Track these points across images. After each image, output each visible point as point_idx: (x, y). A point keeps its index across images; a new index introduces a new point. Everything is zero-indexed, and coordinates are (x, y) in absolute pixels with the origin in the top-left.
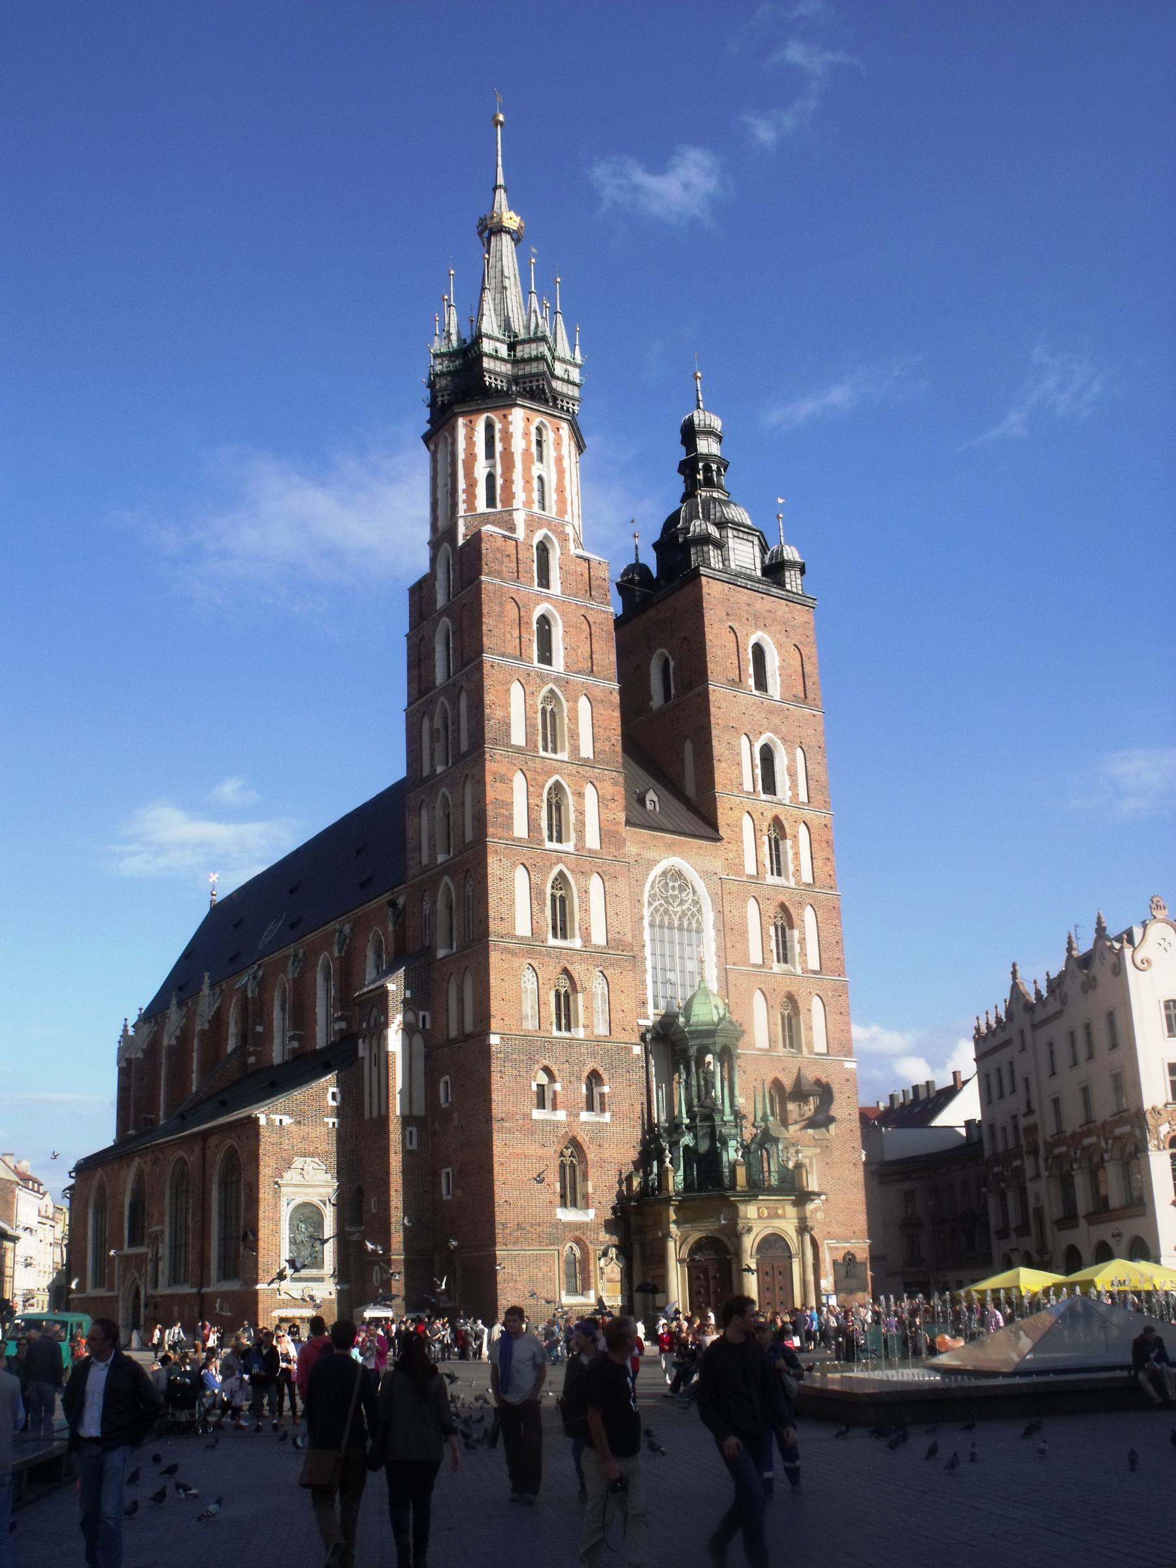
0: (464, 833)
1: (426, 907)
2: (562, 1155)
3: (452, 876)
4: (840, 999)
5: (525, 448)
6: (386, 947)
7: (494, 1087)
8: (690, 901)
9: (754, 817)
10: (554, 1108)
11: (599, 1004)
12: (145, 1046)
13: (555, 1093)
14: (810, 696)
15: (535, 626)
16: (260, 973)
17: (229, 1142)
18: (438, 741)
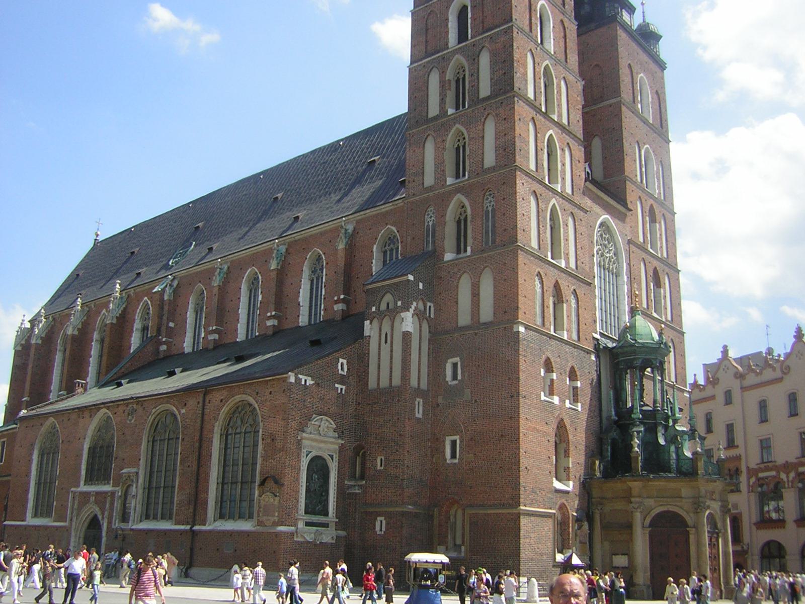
0: (483, 159)
1: (430, 220)
3: (467, 195)
6: (327, 264)
7: (521, 368)
8: (613, 252)
10: (551, 393)
12: (43, 335)
13: (552, 380)
16: (175, 283)
17: (238, 398)
18: (450, 89)
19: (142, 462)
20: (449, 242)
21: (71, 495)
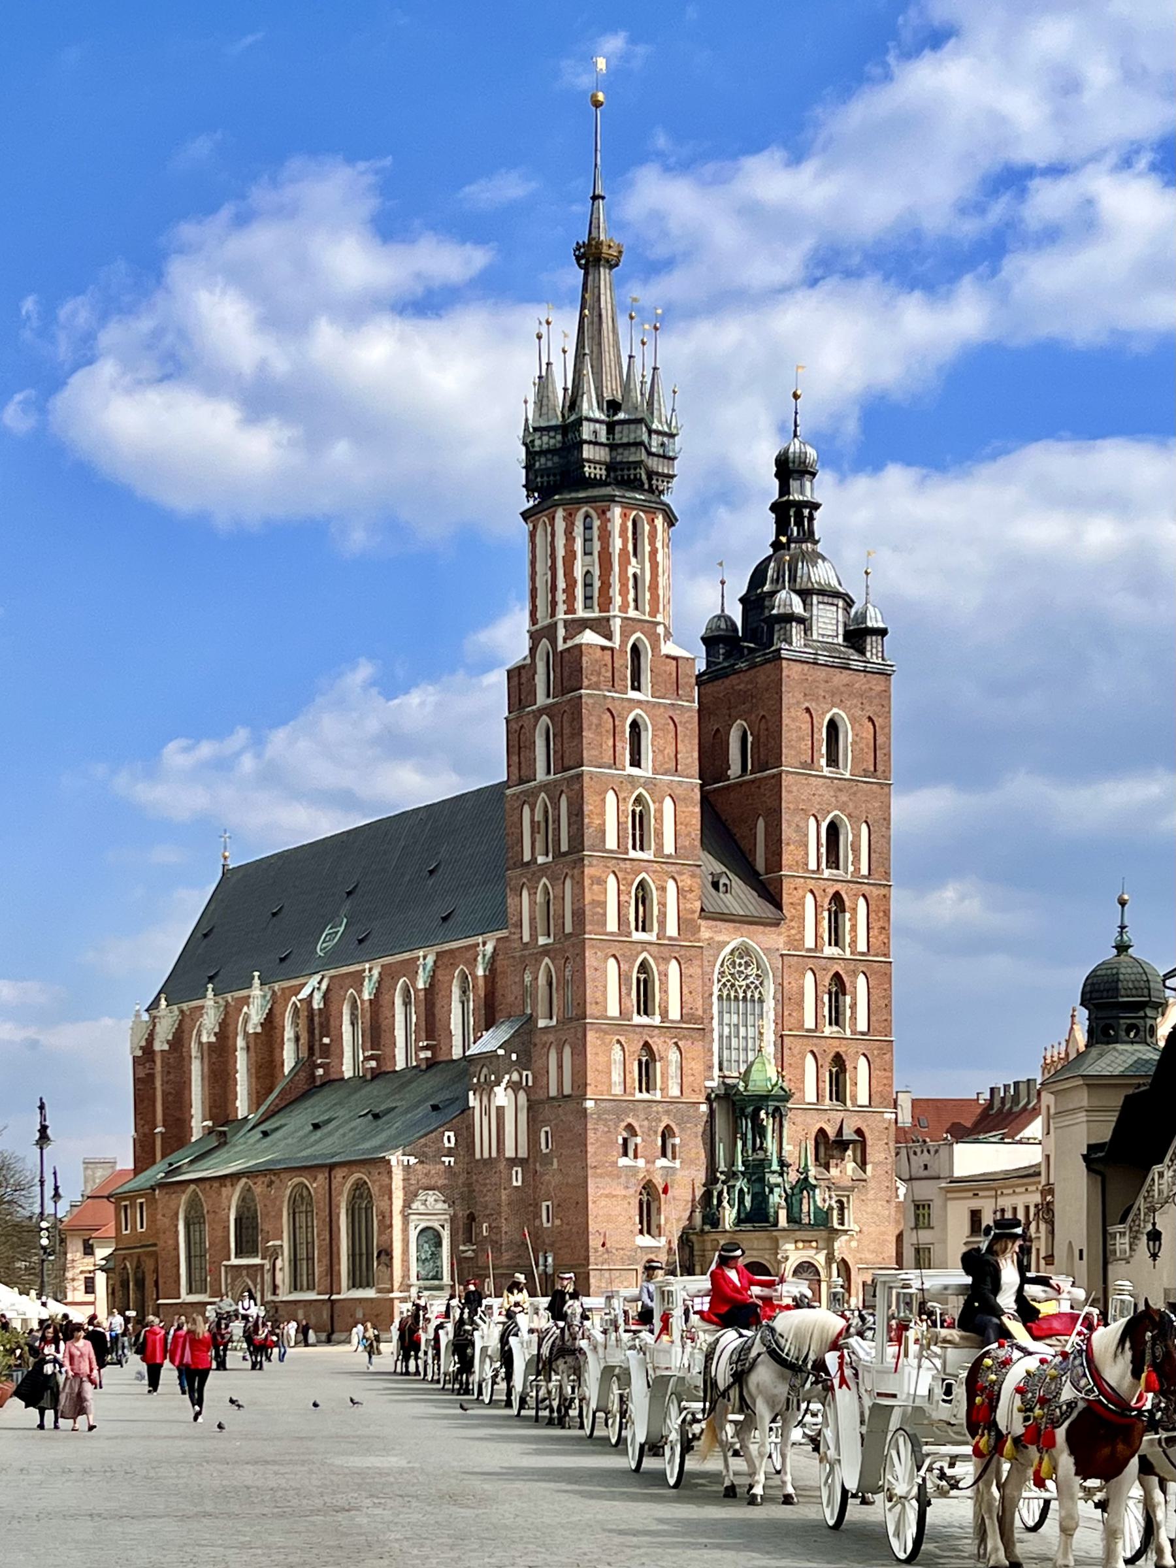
1: (528, 978)
2: (641, 1194)
10: (636, 1157)
11: (673, 1070)
12: (170, 1037)
13: (636, 1145)
14: (880, 768)
15: (627, 735)
16: (324, 986)
19: (285, 1235)
20: (542, 1008)
21: (223, 1269)
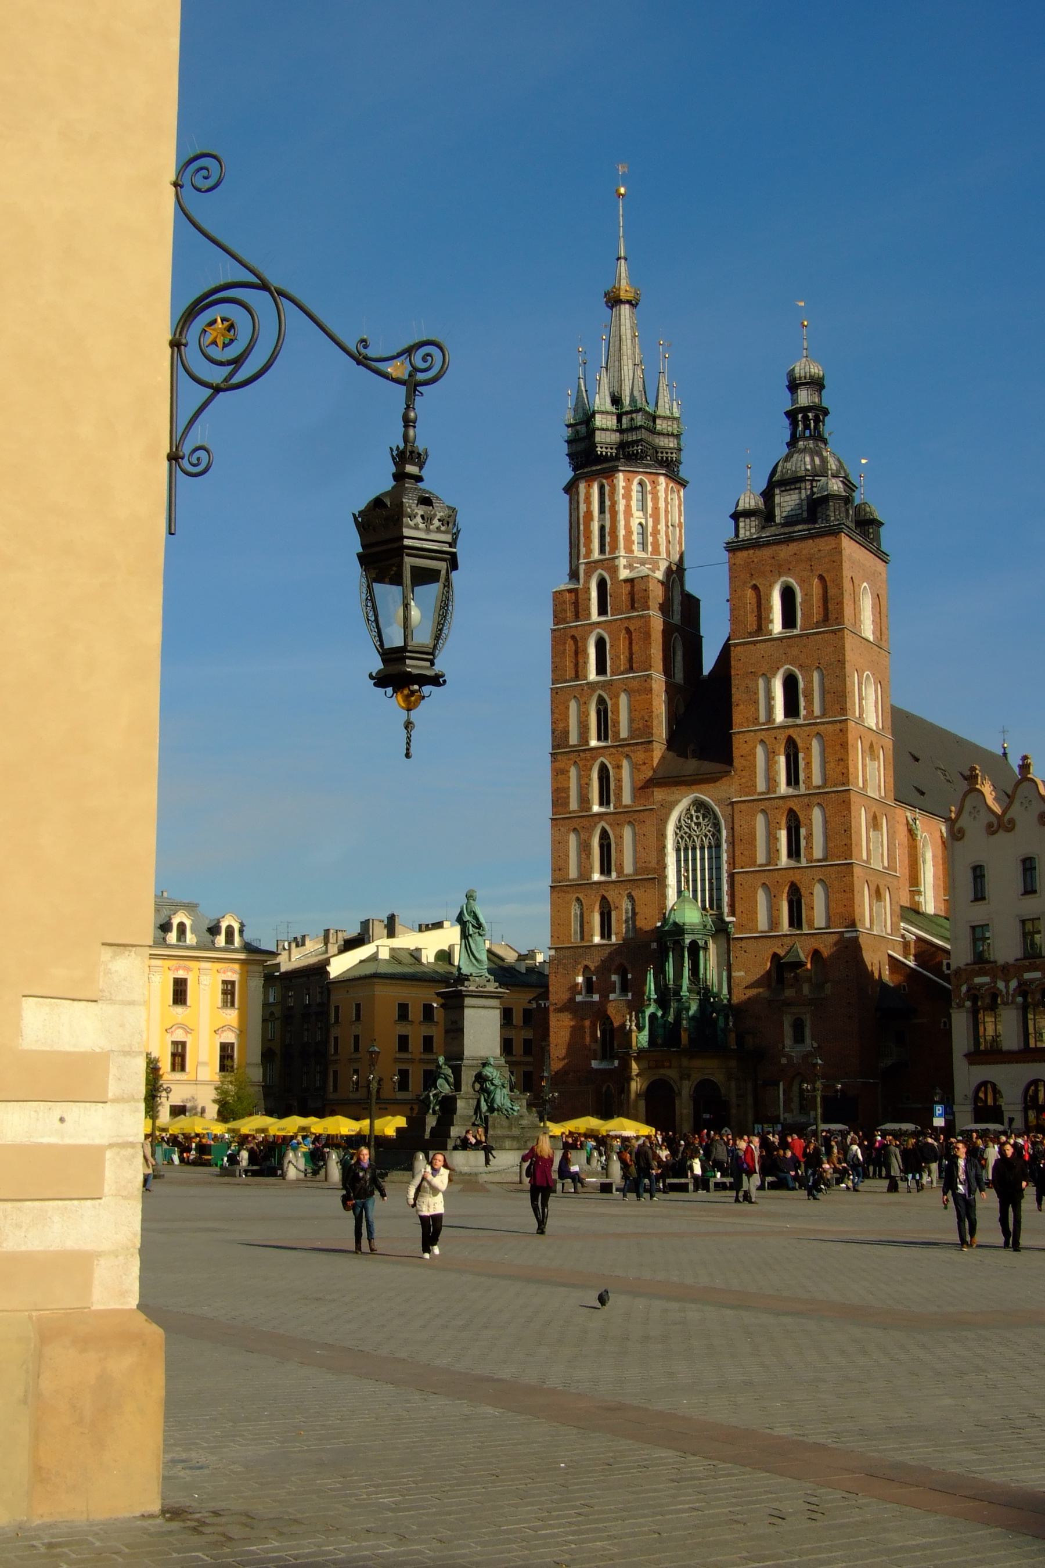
4: (844, 879)
5: (585, 510)
7: (550, 983)
9: (767, 743)
14: (832, 616)
